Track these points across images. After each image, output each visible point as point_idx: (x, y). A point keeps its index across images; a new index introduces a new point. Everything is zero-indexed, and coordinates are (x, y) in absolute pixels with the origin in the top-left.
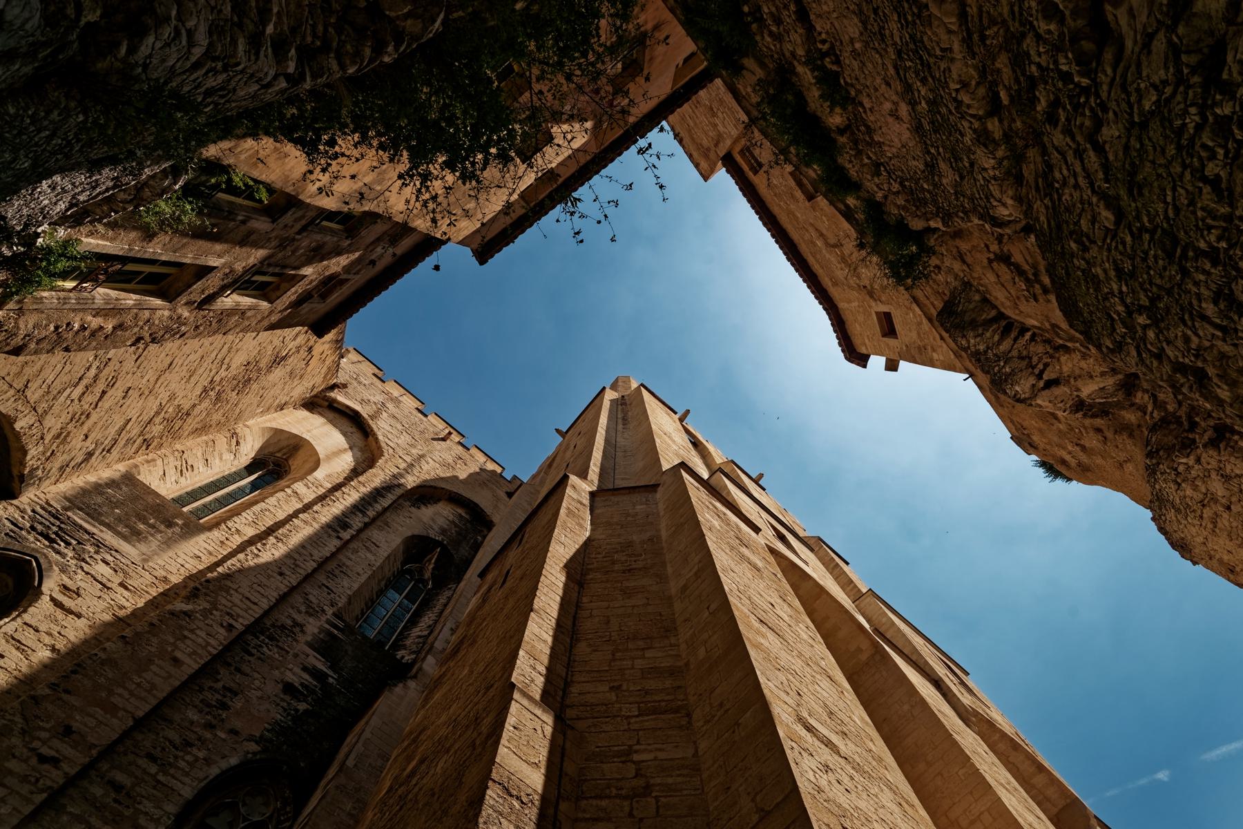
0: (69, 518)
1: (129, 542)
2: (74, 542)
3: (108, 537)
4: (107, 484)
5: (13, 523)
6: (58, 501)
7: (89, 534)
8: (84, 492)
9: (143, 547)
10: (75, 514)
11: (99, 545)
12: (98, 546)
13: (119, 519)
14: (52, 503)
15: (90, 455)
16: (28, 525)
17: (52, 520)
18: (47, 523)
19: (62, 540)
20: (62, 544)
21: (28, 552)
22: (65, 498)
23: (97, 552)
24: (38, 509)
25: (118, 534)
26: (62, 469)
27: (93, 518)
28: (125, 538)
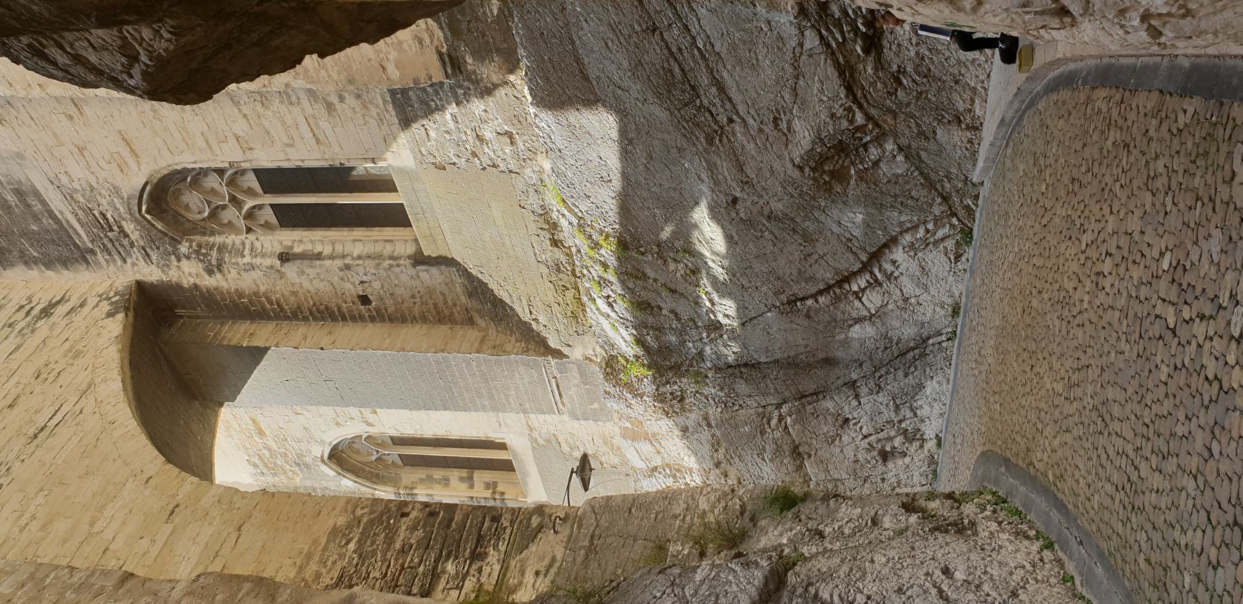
0: (92, 241)
1: (33, 185)
2: (96, 212)
3: (57, 203)
4: (36, 263)
5: (148, 255)
6: (97, 263)
7: (76, 215)
8: (65, 263)
9: (17, 174)
10: (84, 242)
11: (70, 197)
12: (72, 197)
13: (36, 218)
14: (104, 264)
15: (46, 312)
16: (135, 249)
17: (109, 246)
18: (117, 244)
19: (107, 219)
20: (109, 216)
21: (145, 222)
22: (88, 263)
23: (76, 191)
24: (119, 263)
25: (43, 202)
26: (82, 305)
27: (67, 231)
28: (37, 194)
